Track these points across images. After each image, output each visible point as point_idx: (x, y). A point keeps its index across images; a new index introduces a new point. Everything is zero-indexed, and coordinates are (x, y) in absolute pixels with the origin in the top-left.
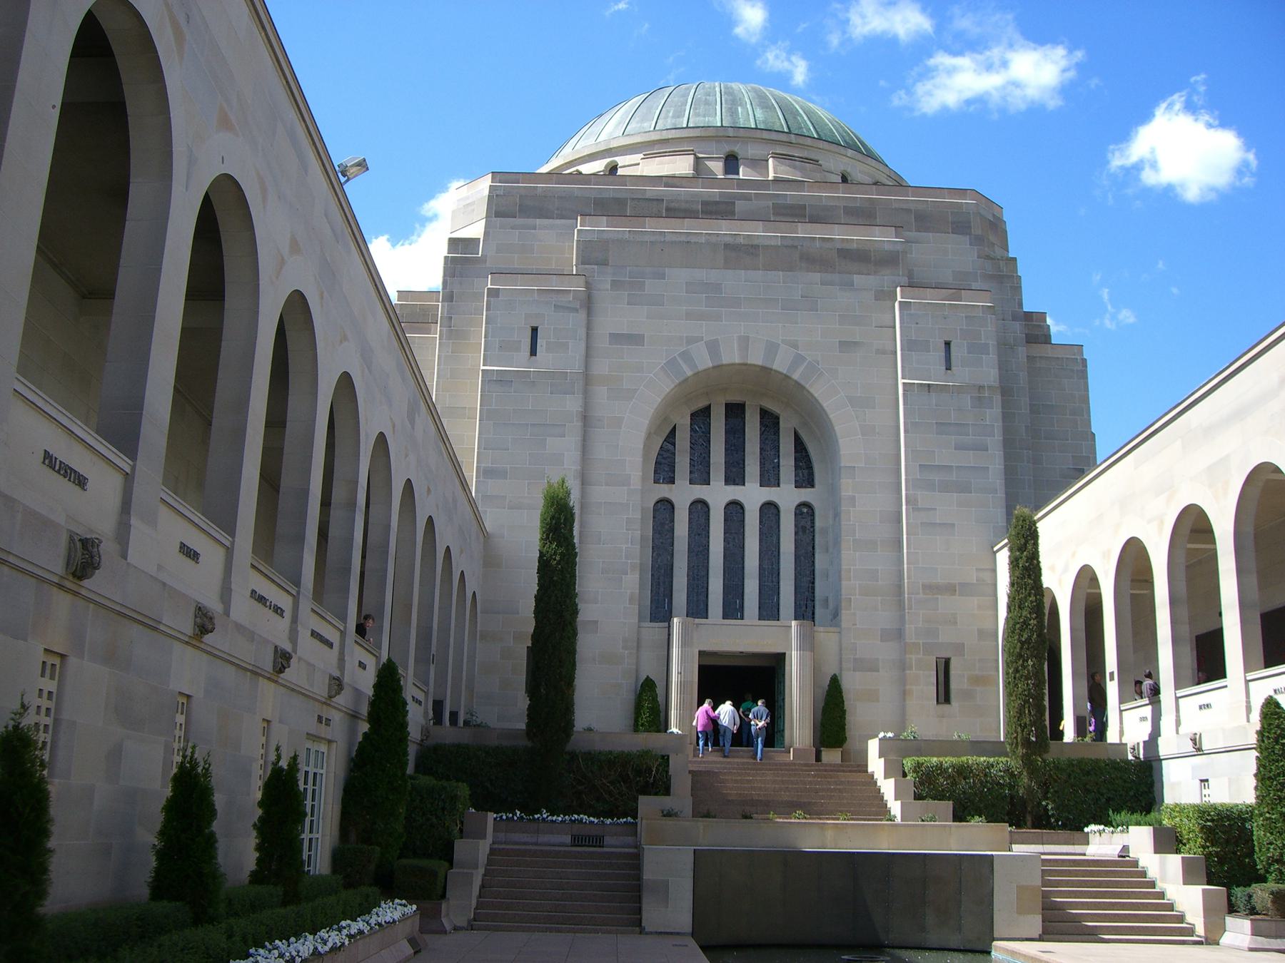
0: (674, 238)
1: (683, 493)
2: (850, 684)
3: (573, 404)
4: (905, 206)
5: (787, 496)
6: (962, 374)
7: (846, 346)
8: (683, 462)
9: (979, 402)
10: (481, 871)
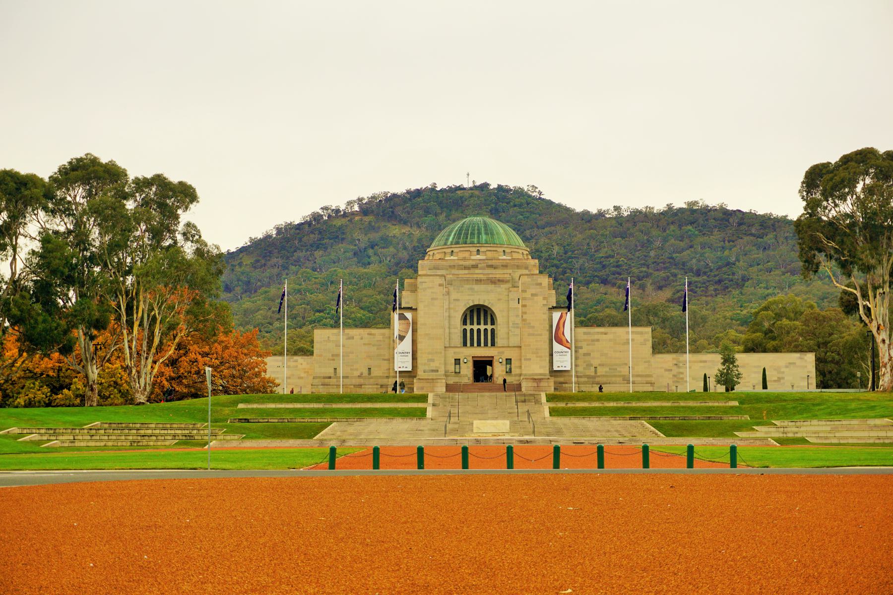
1: (468, 327)
7: (499, 300)
8: (468, 321)
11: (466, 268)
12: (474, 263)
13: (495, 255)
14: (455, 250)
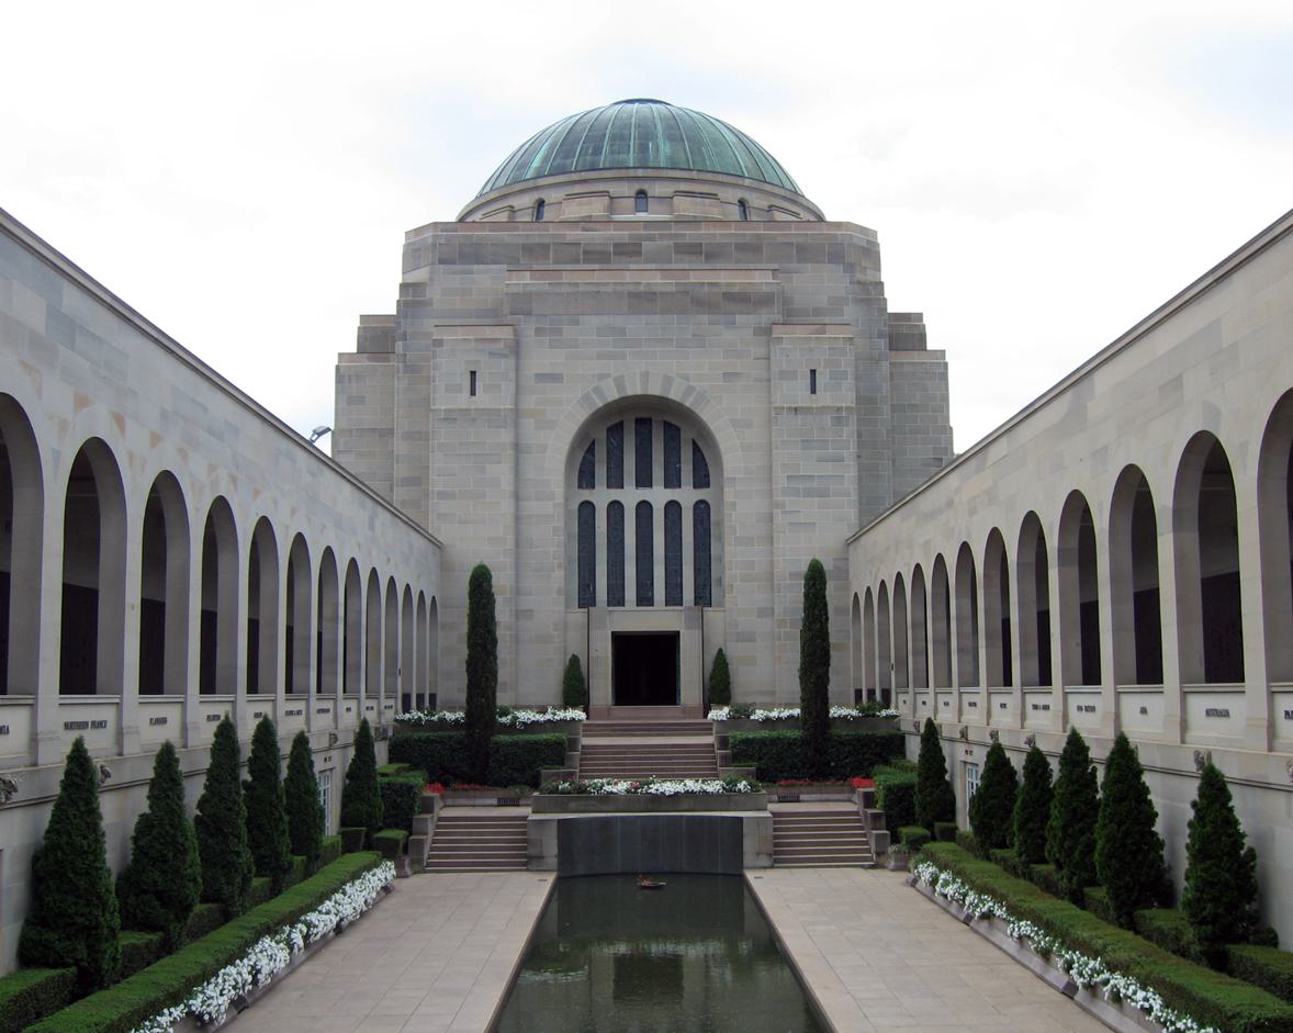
0: (588, 289)
1: (601, 497)
2: (734, 652)
3: (506, 436)
4: (786, 240)
5: (687, 496)
6: (824, 398)
7: (728, 376)
8: (601, 472)
9: (838, 421)
10: (430, 837)
11: (596, 256)
12: (623, 235)
13: (715, 212)
14: (551, 196)
